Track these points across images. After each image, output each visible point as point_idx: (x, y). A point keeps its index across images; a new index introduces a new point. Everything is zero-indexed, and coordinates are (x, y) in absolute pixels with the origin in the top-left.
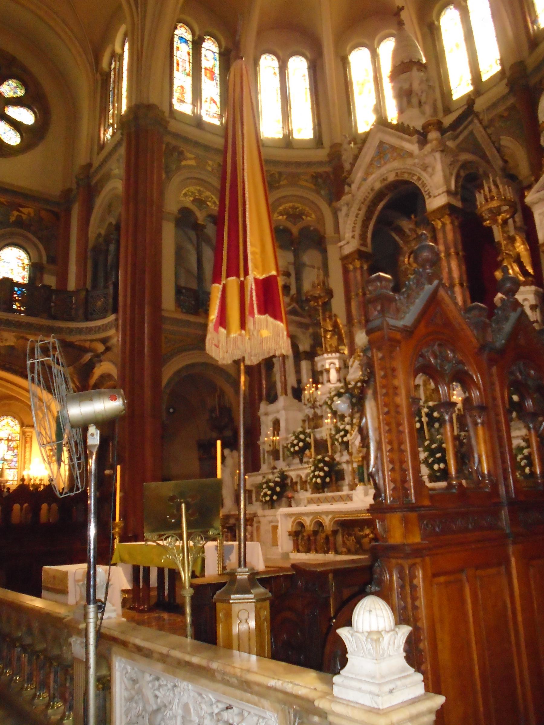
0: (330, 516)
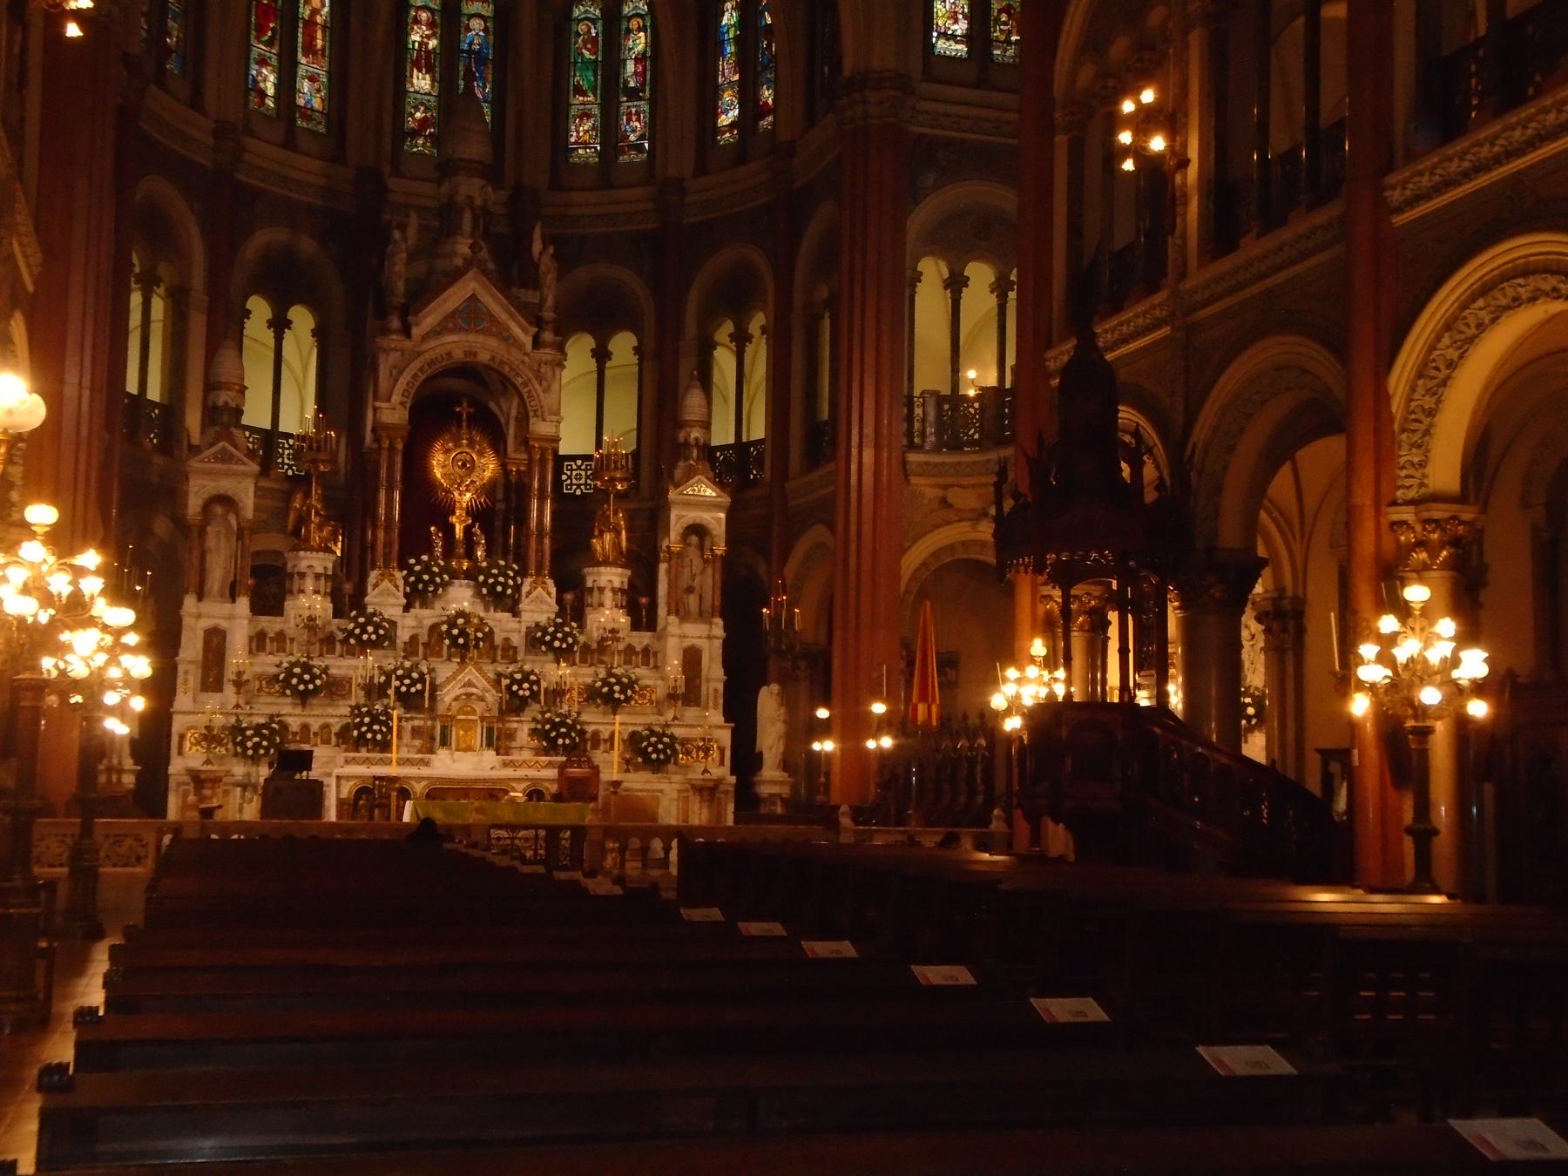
0: (423, 784)
